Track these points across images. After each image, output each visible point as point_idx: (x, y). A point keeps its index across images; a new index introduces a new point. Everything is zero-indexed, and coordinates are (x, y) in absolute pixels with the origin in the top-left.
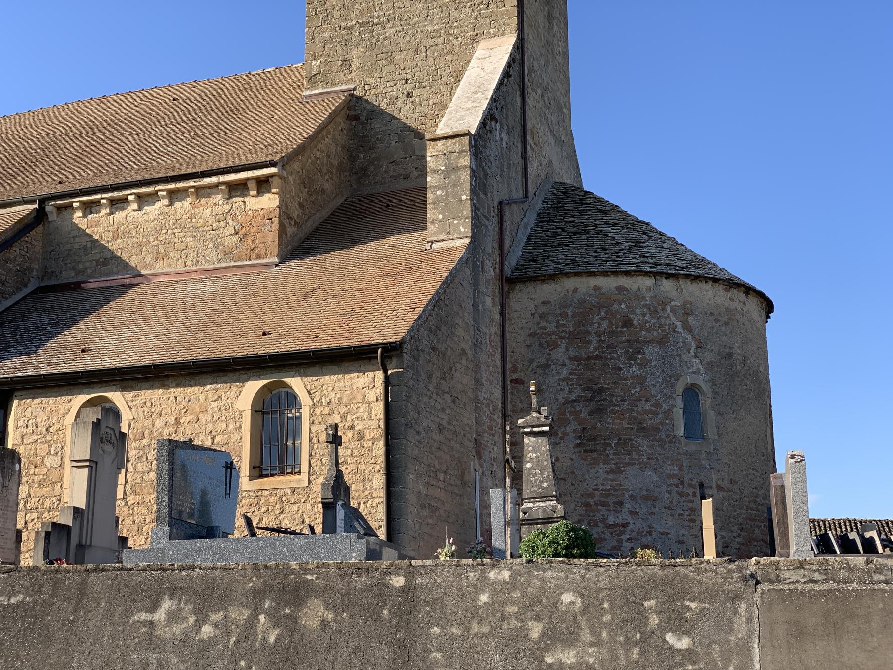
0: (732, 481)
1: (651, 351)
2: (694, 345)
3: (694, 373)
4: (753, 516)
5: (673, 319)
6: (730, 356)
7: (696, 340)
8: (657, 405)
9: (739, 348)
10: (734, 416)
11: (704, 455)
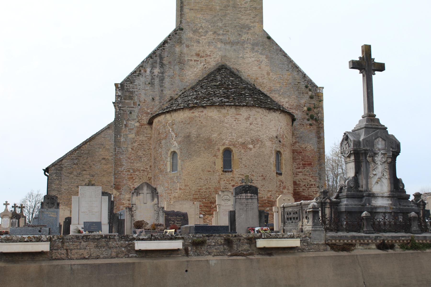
0: (186, 186)
1: (163, 142)
2: (175, 136)
3: (174, 147)
4: (197, 198)
5: (169, 128)
6: (189, 136)
7: (176, 134)
8: (164, 162)
9: (195, 132)
10: (189, 160)
11: (176, 177)
